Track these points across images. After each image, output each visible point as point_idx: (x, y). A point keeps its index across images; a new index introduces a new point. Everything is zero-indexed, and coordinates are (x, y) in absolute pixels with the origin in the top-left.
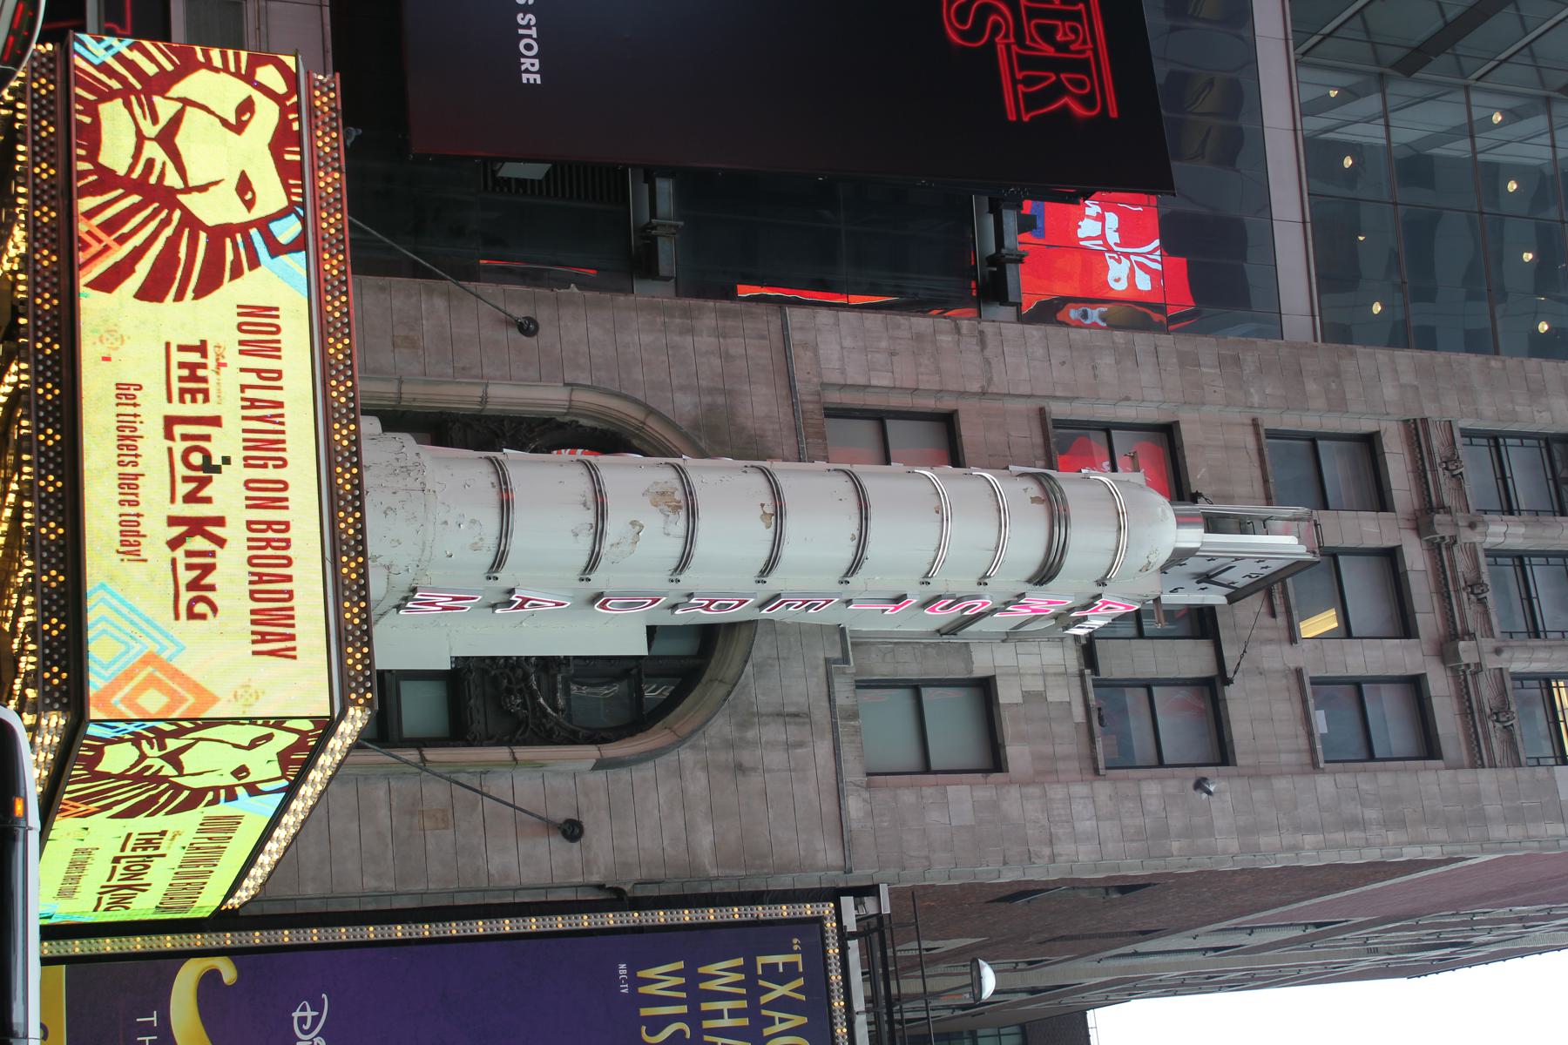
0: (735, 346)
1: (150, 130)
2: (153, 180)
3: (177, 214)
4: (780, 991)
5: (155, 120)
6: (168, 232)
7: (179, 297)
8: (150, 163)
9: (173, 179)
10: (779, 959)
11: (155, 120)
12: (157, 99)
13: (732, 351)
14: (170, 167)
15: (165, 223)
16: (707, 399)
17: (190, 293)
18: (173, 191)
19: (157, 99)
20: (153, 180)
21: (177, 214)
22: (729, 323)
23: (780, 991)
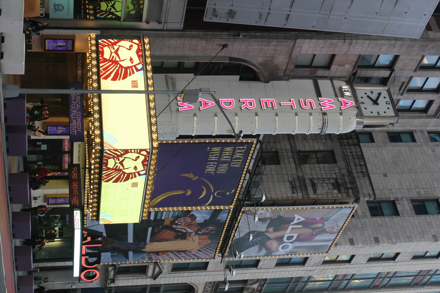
0: (279, 48)
1: (113, 51)
2: (114, 60)
3: (118, 65)
4: (240, 151)
5: (114, 49)
6: (117, 68)
7: (119, 80)
8: (113, 57)
9: (118, 59)
10: (241, 147)
11: (114, 49)
12: (114, 46)
13: (278, 49)
14: (117, 57)
15: (116, 67)
16: (266, 59)
17: (121, 79)
18: (118, 61)
19: (114, 46)
20: (114, 60)
21: (118, 65)
22: (280, 44)
23: (240, 151)
